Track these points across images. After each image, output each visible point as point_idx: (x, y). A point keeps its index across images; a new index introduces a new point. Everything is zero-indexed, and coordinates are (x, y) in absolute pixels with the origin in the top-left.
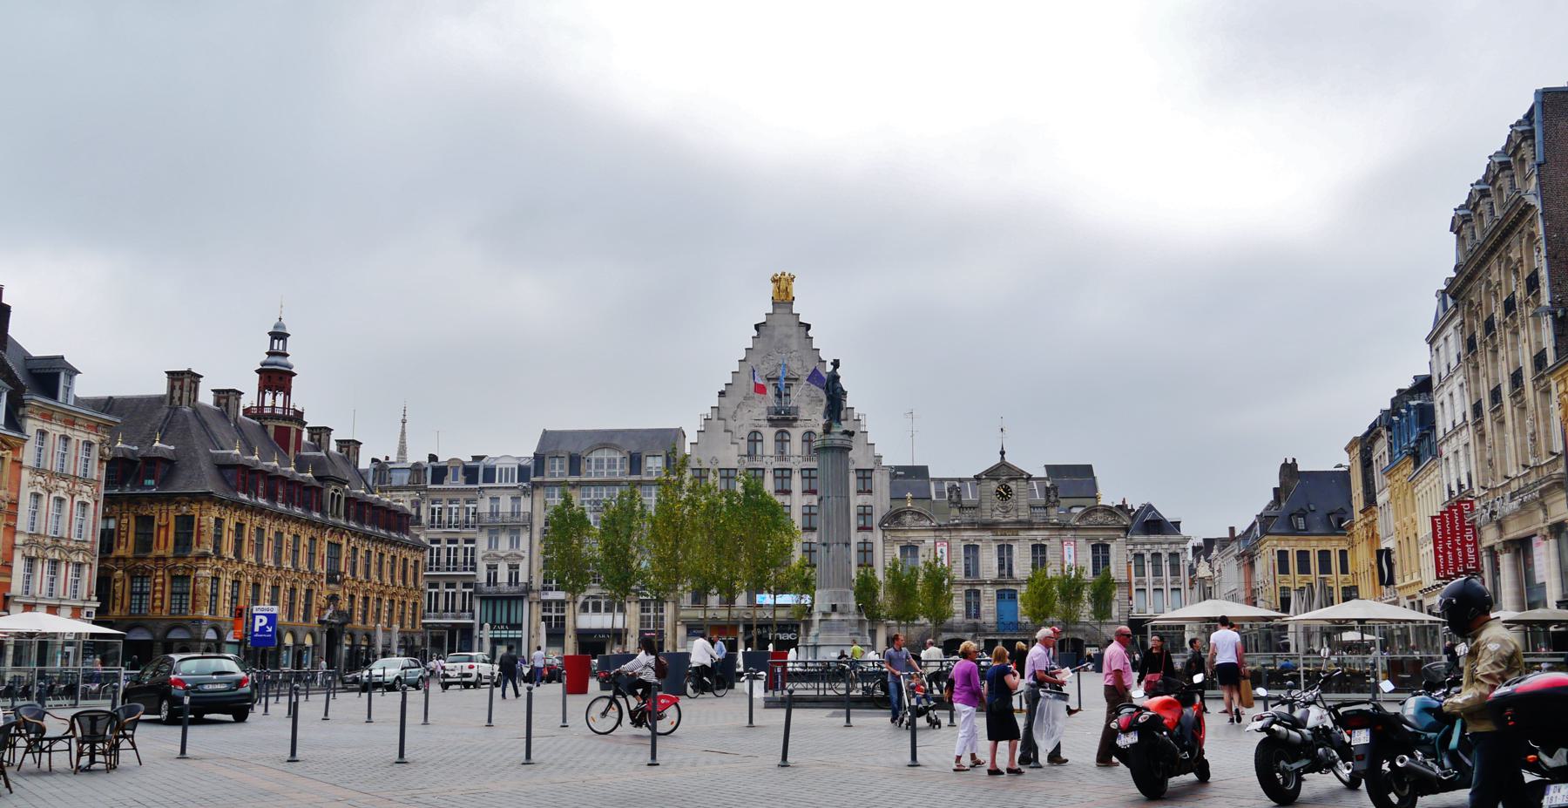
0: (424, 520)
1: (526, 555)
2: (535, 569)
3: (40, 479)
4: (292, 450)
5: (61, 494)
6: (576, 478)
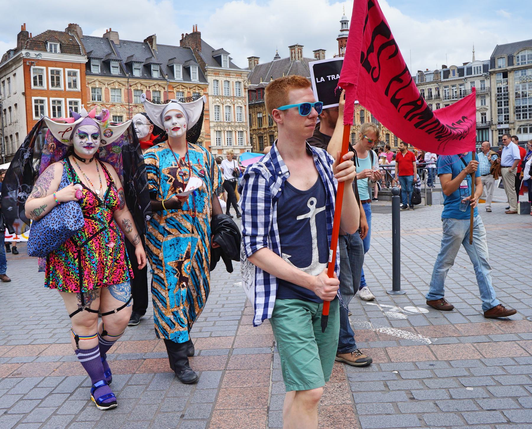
0: (441, 96)
1: (489, 108)
2: (493, 115)
3: (217, 99)
5: (228, 104)
6: (511, 67)
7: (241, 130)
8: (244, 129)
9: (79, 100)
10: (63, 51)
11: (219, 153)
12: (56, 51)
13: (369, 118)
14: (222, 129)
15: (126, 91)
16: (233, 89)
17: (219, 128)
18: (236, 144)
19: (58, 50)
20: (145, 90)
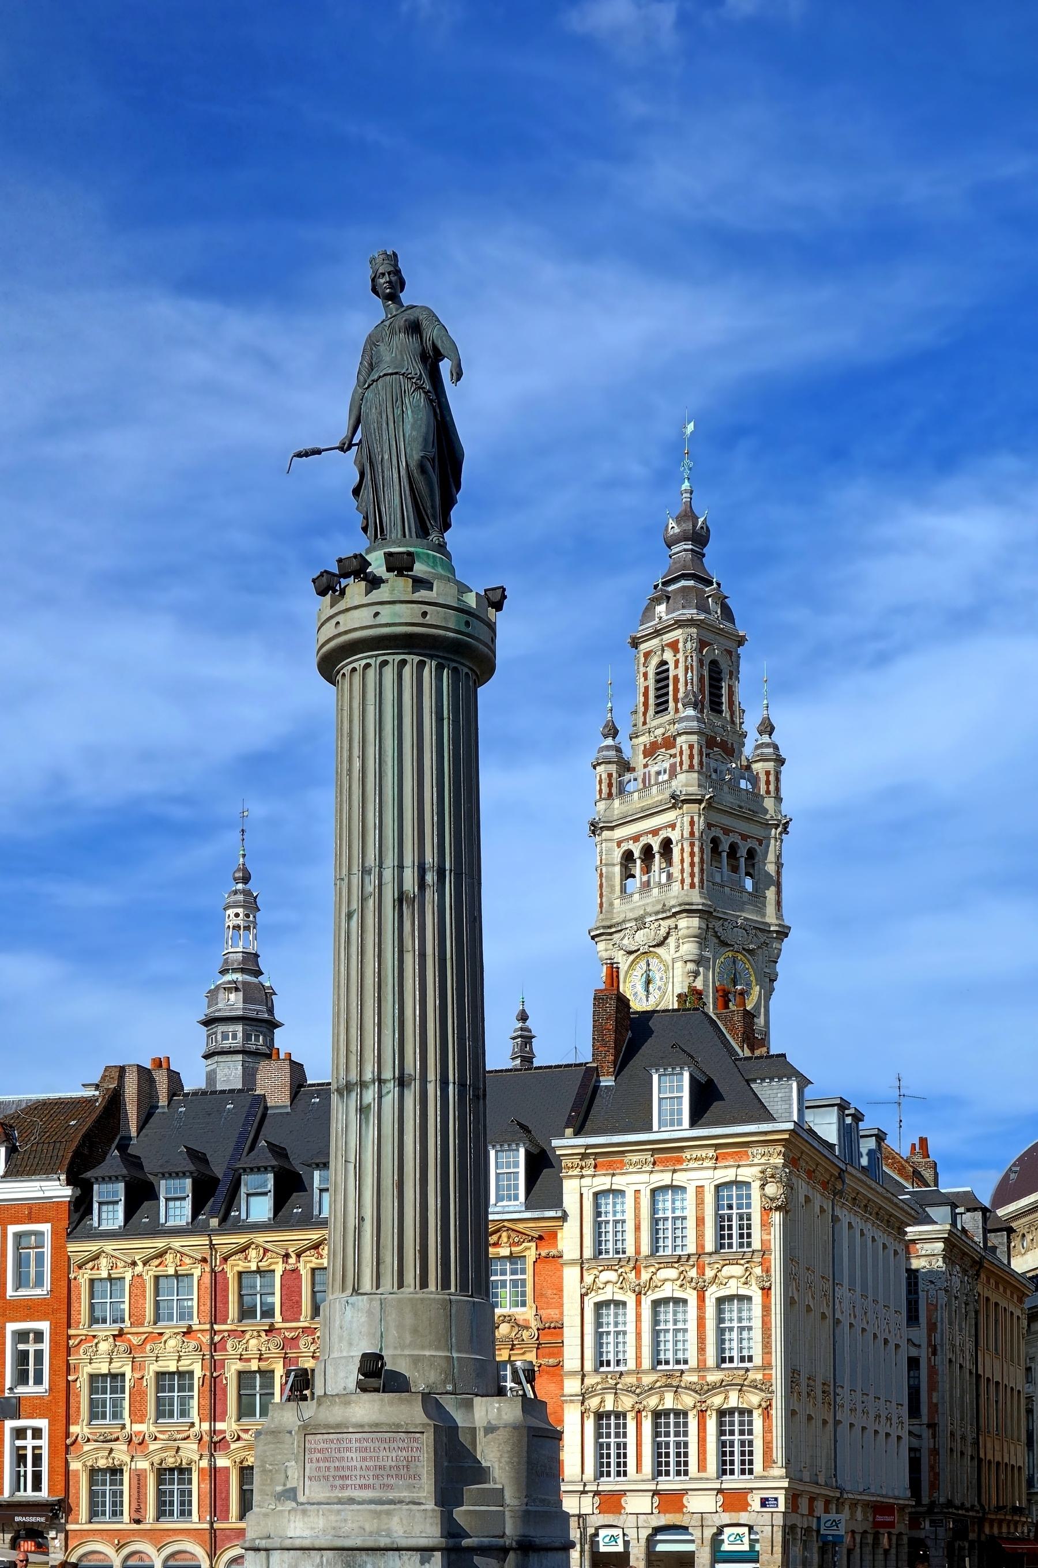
7: (733, 1400)
8: (754, 1399)
9: (44, 1326)
11: (603, 1509)
14: (627, 1402)
15: (207, 1279)
16: (700, 1221)
17: (609, 1399)
18: (702, 1466)
20: (279, 1269)
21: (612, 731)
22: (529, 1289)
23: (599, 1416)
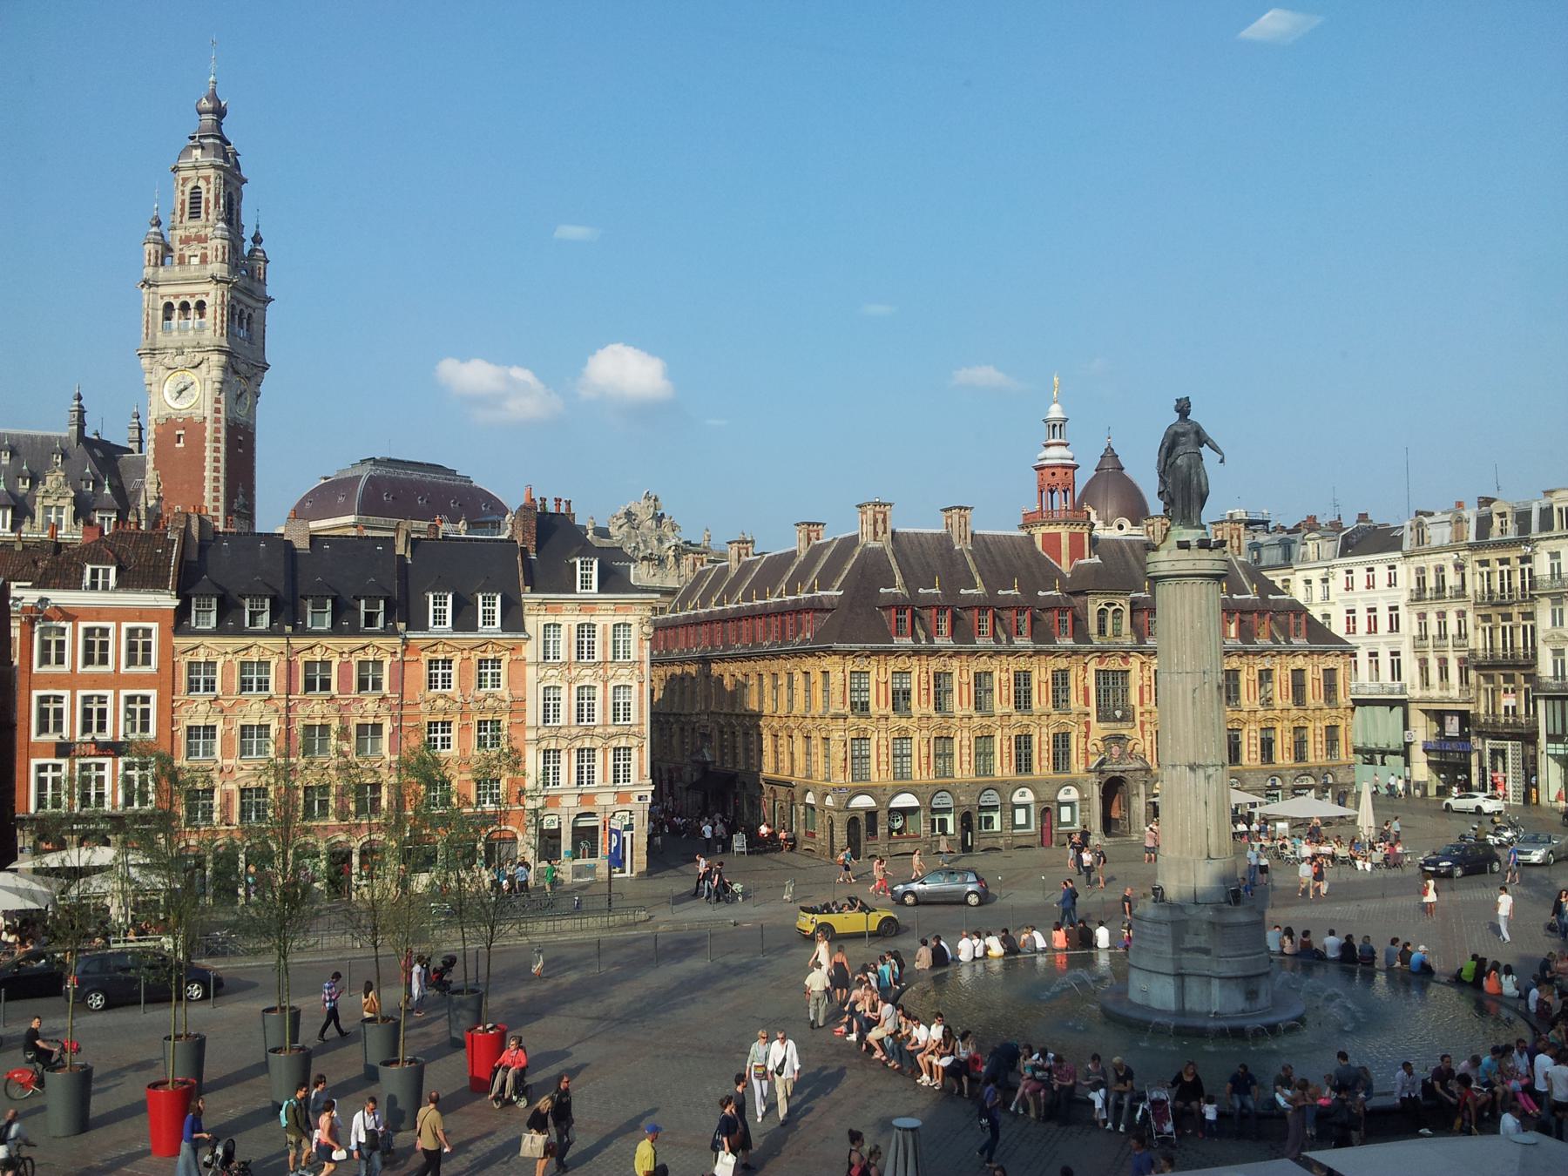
4: (1065, 560)
5: (586, 682)
7: (623, 743)
8: (634, 742)
9: (153, 693)
10: (124, 583)
12: (105, 587)
13: (1086, 690)
15: (284, 665)
19: (112, 581)
21: (158, 224)
22: (503, 678)
23: (546, 752)
